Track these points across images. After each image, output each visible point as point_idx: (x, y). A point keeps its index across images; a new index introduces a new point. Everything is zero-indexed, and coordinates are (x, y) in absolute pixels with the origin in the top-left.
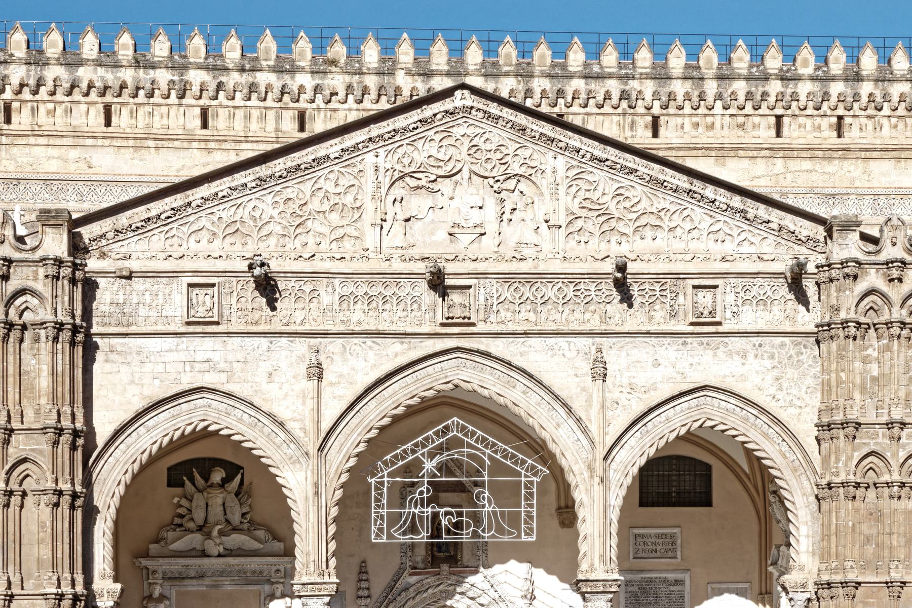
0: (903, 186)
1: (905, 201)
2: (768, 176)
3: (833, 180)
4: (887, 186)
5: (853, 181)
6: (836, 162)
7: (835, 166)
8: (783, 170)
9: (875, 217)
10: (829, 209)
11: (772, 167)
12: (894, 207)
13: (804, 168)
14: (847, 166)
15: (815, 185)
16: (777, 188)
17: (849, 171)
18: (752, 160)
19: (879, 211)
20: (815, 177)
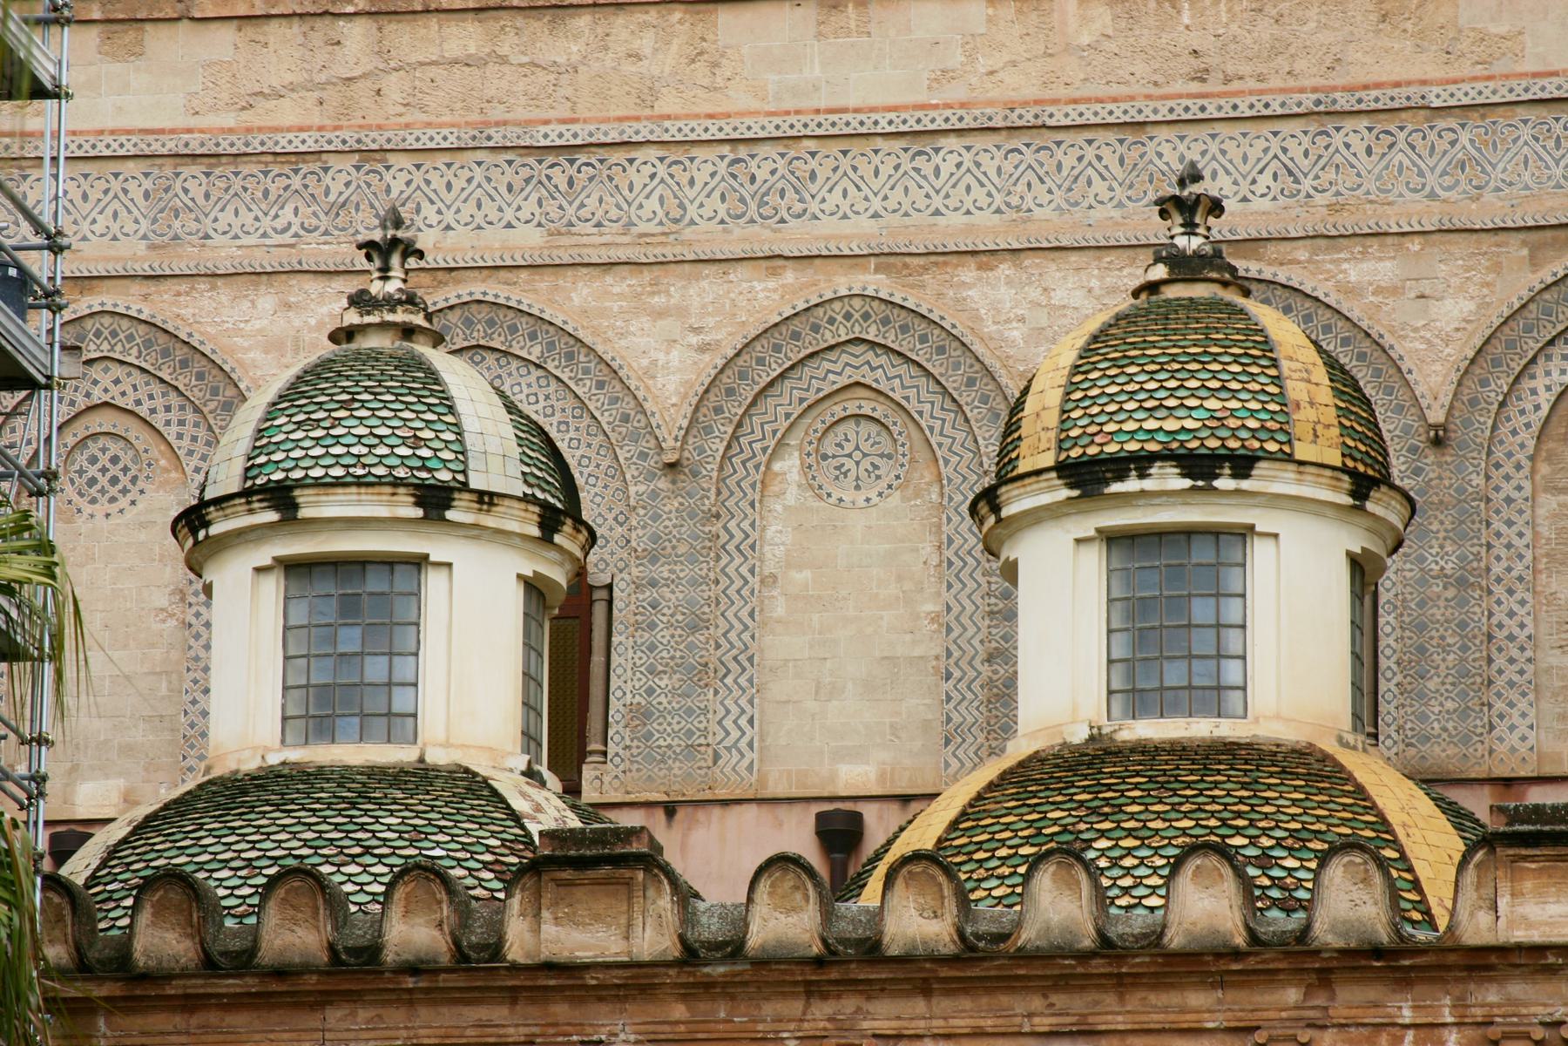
0: (852, 103)
1: (861, 163)
2: (310, 86)
3: (569, 92)
4: (789, 105)
5: (649, 93)
6: (583, 21)
7: (576, 37)
8: (367, 64)
9: (738, 230)
10: (551, 207)
11: (321, 57)
12: (814, 188)
13: (453, 49)
14: (624, 35)
15: (497, 113)
16: (345, 134)
17: (636, 56)
18: (250, 31)
19: (753, 206)
20: (496, 81)
